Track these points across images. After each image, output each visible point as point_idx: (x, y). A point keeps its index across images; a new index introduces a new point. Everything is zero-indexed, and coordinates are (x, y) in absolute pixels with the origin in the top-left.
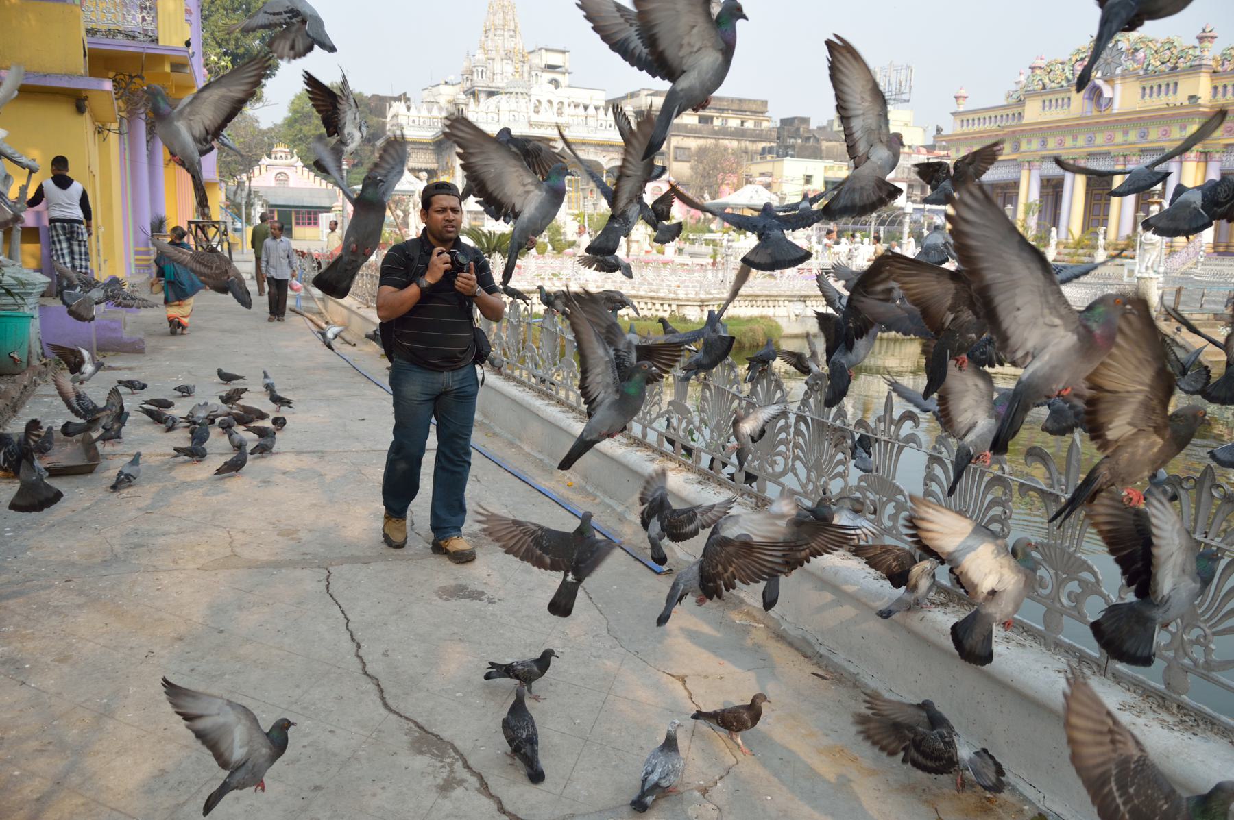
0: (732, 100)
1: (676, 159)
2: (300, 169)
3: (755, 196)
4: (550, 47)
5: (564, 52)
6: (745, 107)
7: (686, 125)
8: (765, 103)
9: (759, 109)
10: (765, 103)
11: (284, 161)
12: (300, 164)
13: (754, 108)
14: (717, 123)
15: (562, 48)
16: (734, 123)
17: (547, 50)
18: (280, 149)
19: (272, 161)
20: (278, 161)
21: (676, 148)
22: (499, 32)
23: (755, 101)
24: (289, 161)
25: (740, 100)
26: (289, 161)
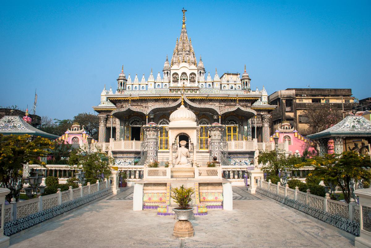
0: (331, 90)
1: (300, 122)
2: (84, 135)
3: (358, 126)
4: (229, 73)
5: (237, 75)
6: (338, 93)
7: (305, 104)
8: (350, 90)
9: (347, 93)
10: (350, 90)
11: (77, 131)
12: (85, 132)
13: (344, 93)
14: (323, 102)
15: (236, 73)
16: (333, 101)
17: (228, 74)
18: (76, 126)
19: (71, 132)
20: (74, 132)
21: (300, 116)
22: (180, 53)
23: (344, 90)
24: (79, 131)
25: (335, 90)
26: (79, 131)
